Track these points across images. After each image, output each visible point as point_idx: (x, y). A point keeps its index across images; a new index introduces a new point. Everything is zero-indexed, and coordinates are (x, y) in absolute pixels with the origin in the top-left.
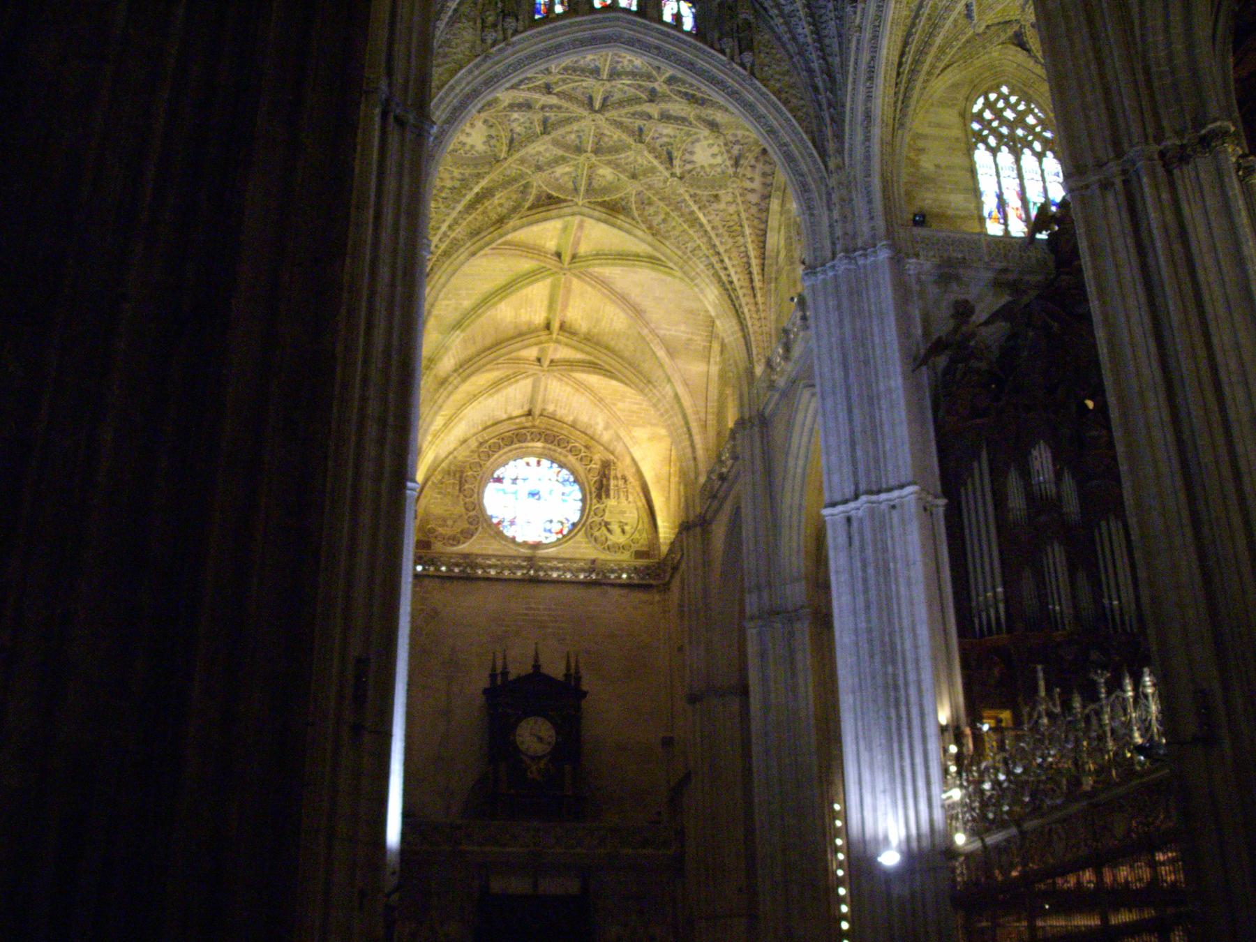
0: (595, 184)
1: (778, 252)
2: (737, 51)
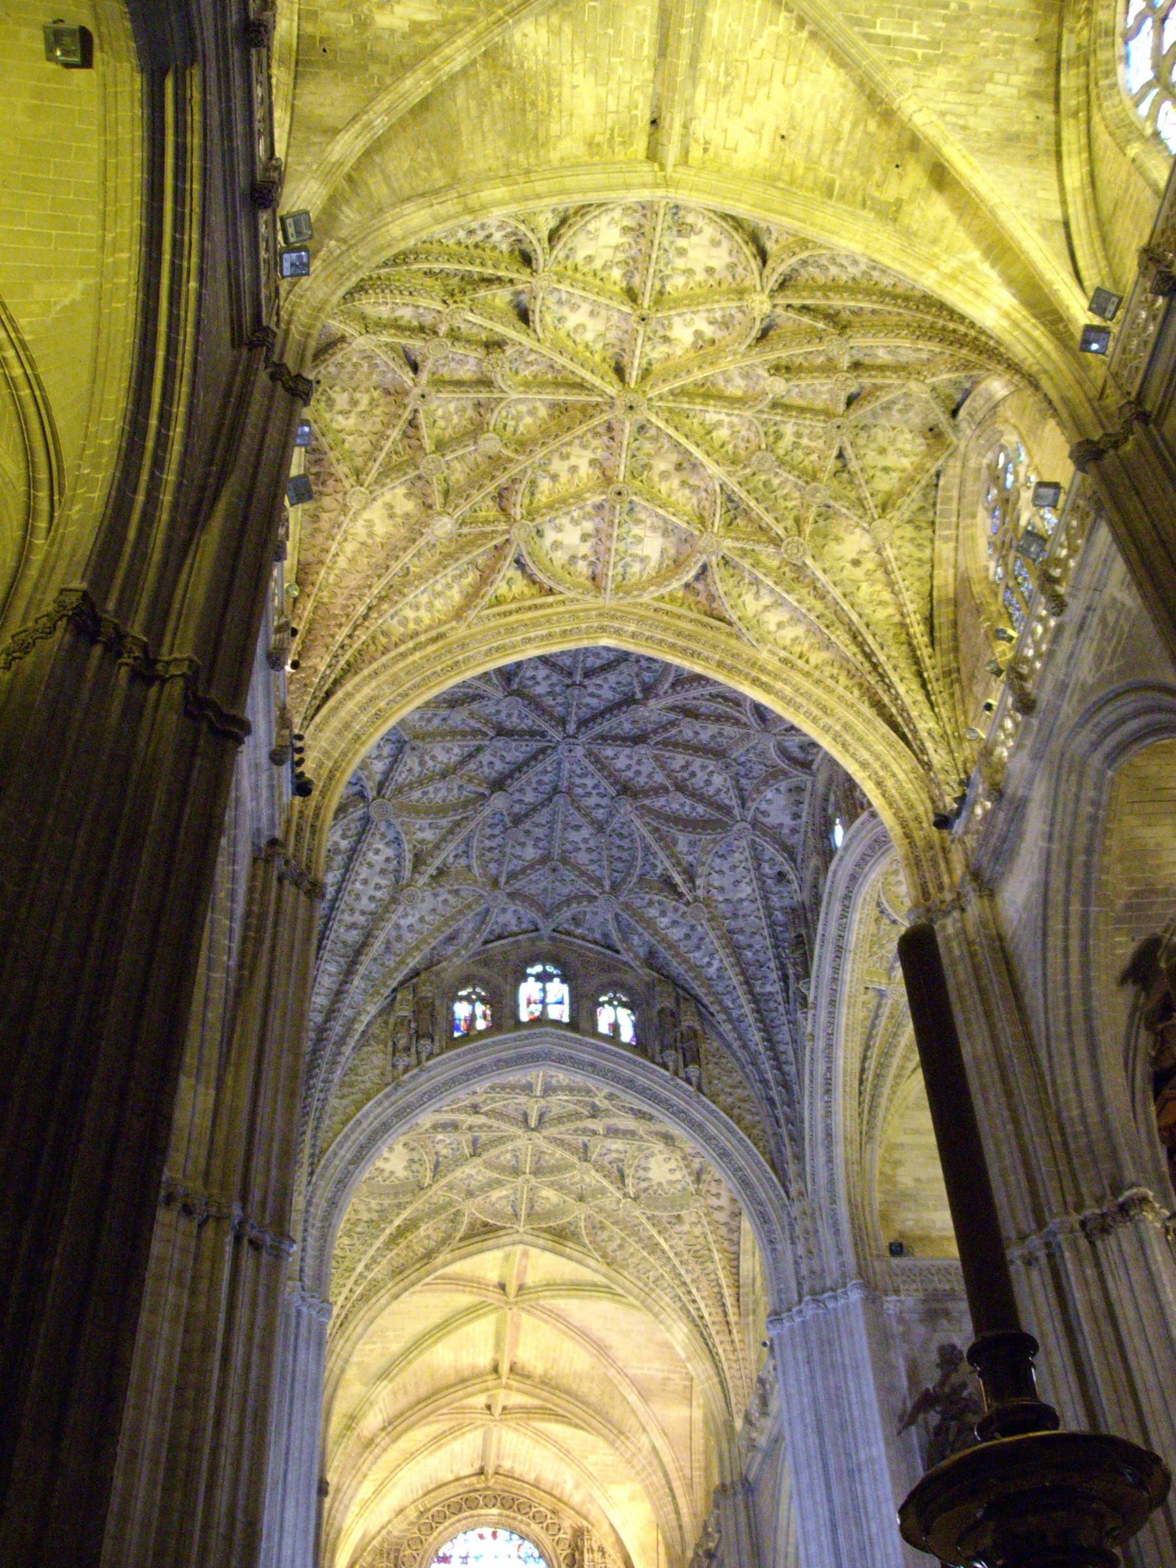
0: (537, 1208)
1: (754, 1279)
2: (681, 1064)
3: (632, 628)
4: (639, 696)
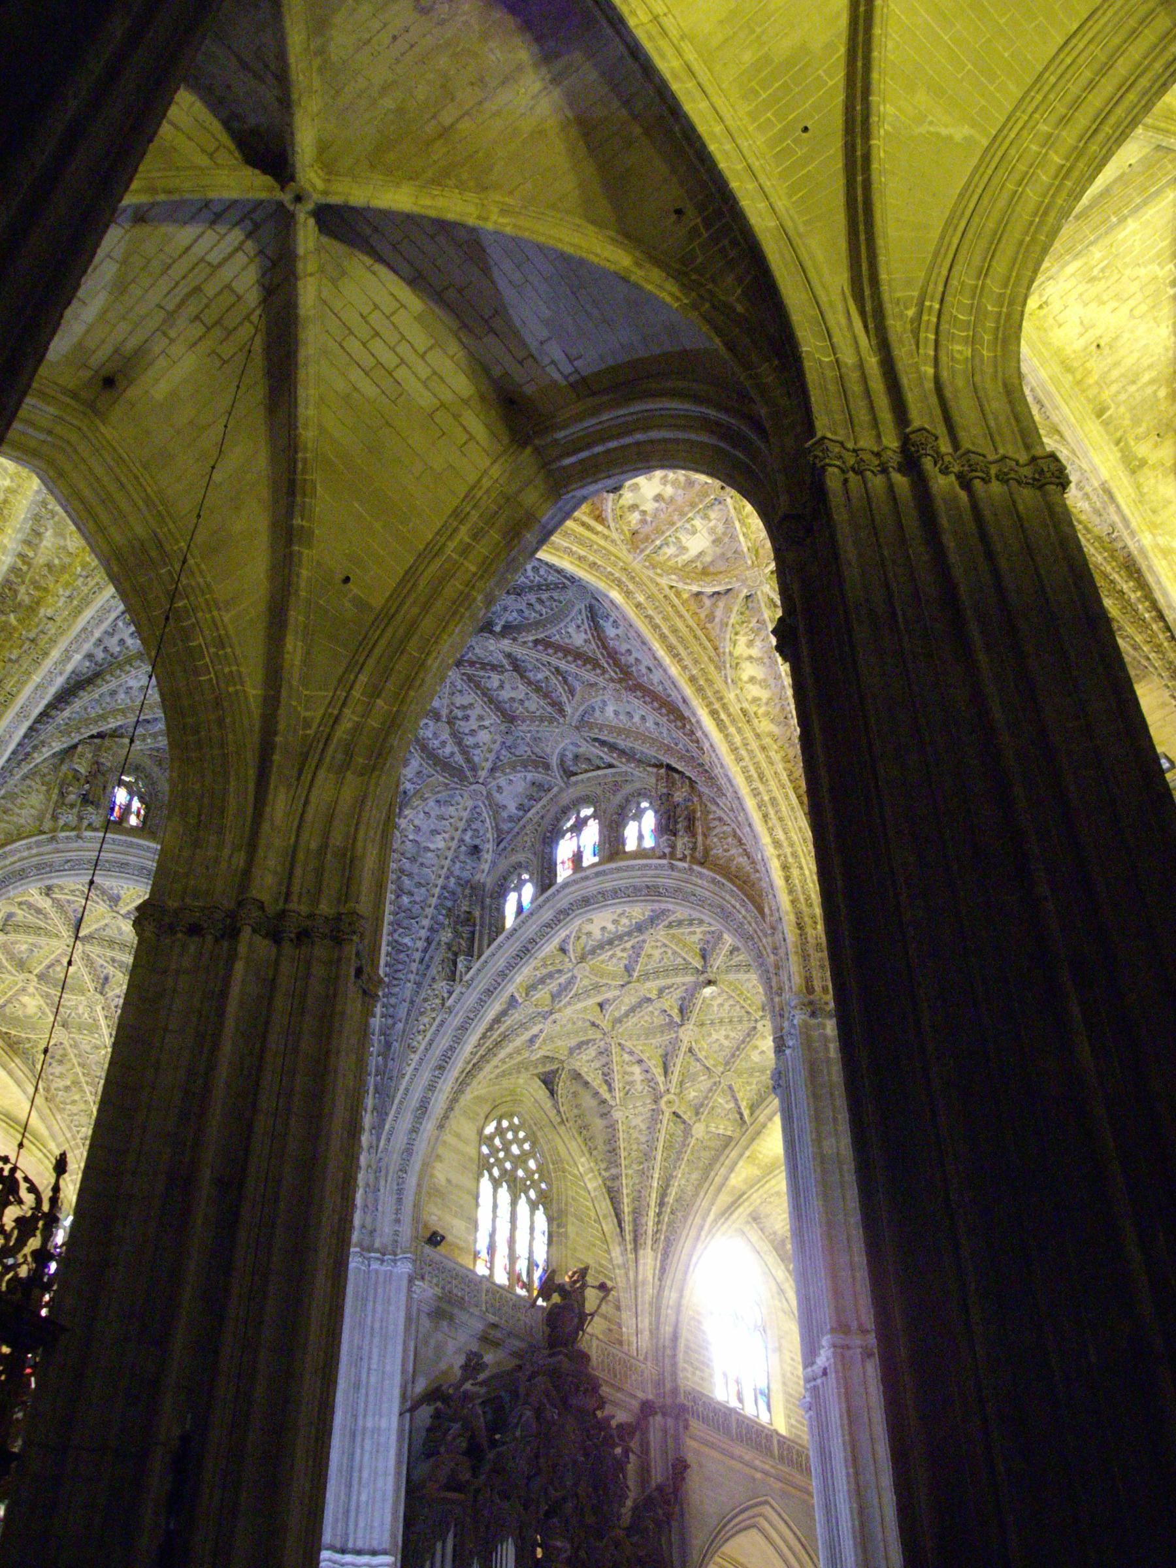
3: (641, 598)
4: (498, 629)
